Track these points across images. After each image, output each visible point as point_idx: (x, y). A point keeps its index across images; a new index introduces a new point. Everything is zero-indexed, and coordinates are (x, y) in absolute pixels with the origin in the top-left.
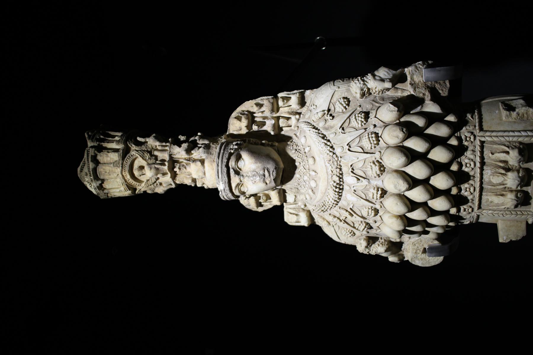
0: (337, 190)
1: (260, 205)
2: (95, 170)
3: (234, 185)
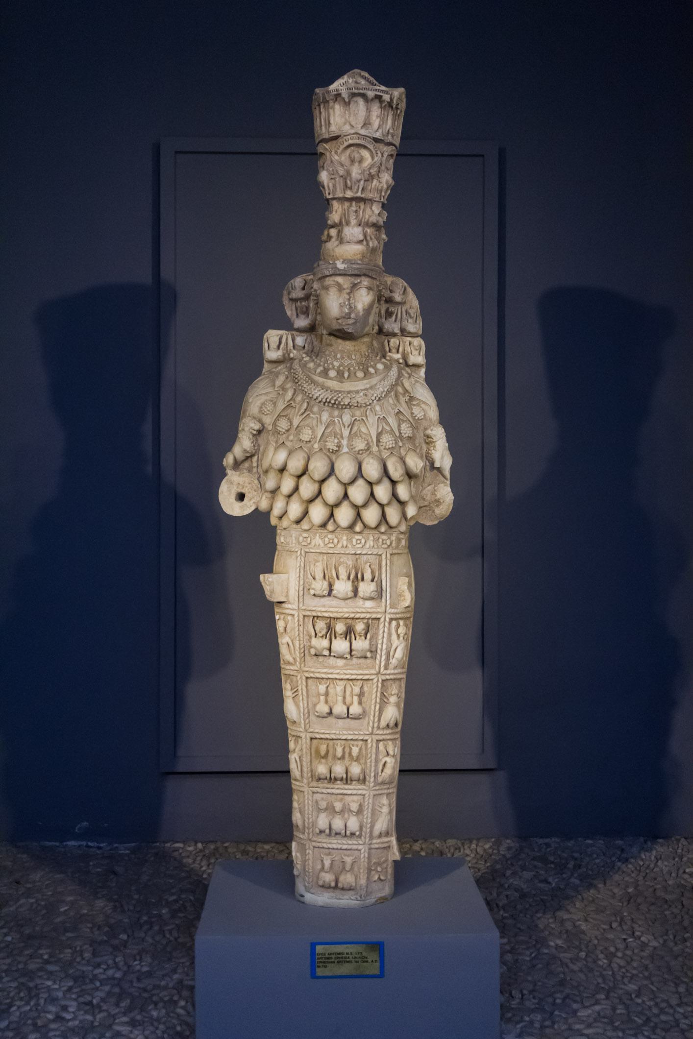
0: (333, 402)
1: (293, 300)
2: (363, 96)
3: (340, 279)
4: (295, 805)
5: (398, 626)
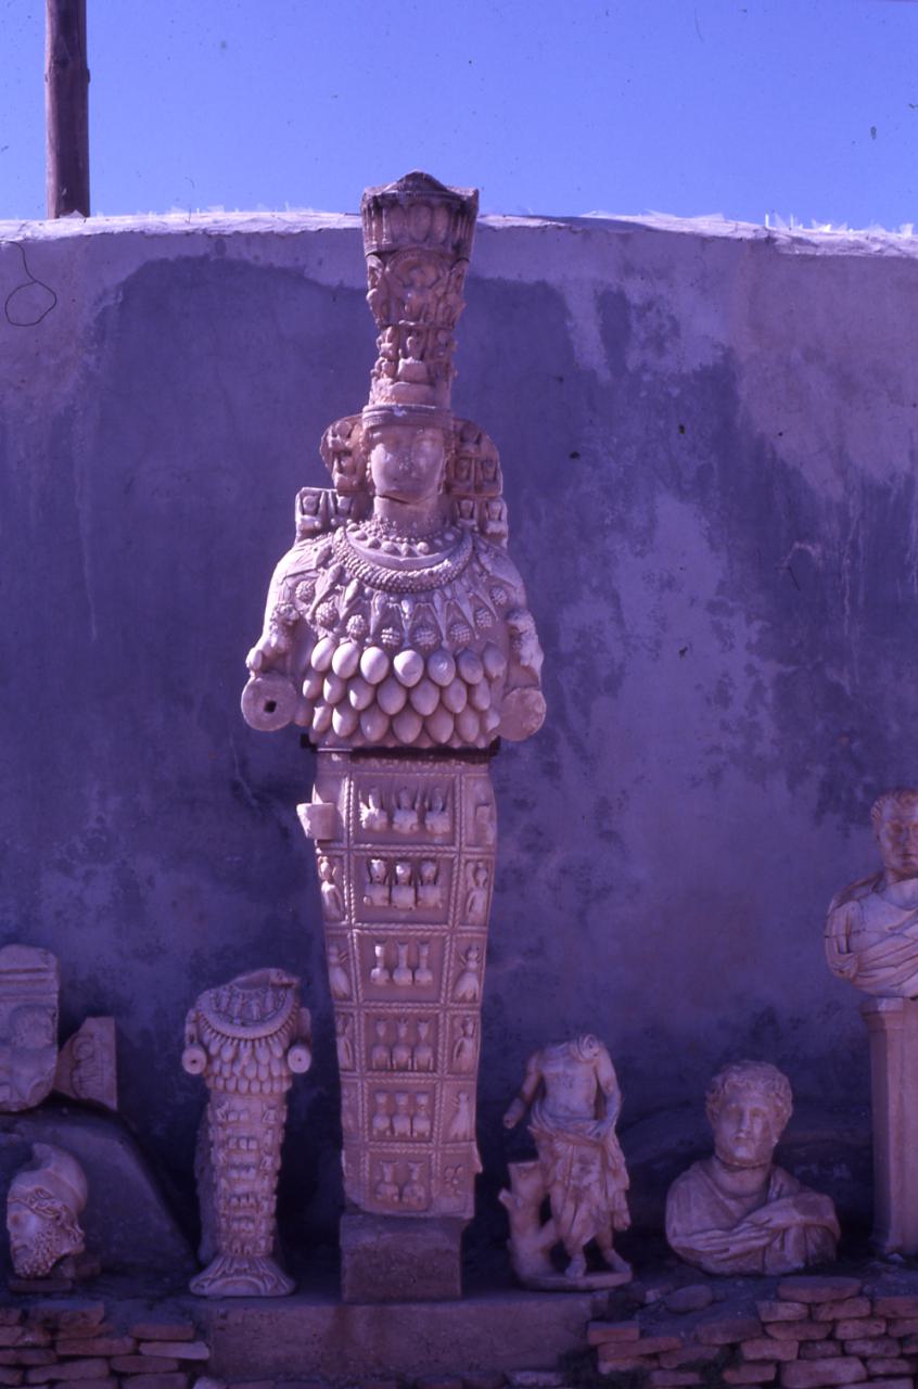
4: (345, 1102)
5: (477, 870)
